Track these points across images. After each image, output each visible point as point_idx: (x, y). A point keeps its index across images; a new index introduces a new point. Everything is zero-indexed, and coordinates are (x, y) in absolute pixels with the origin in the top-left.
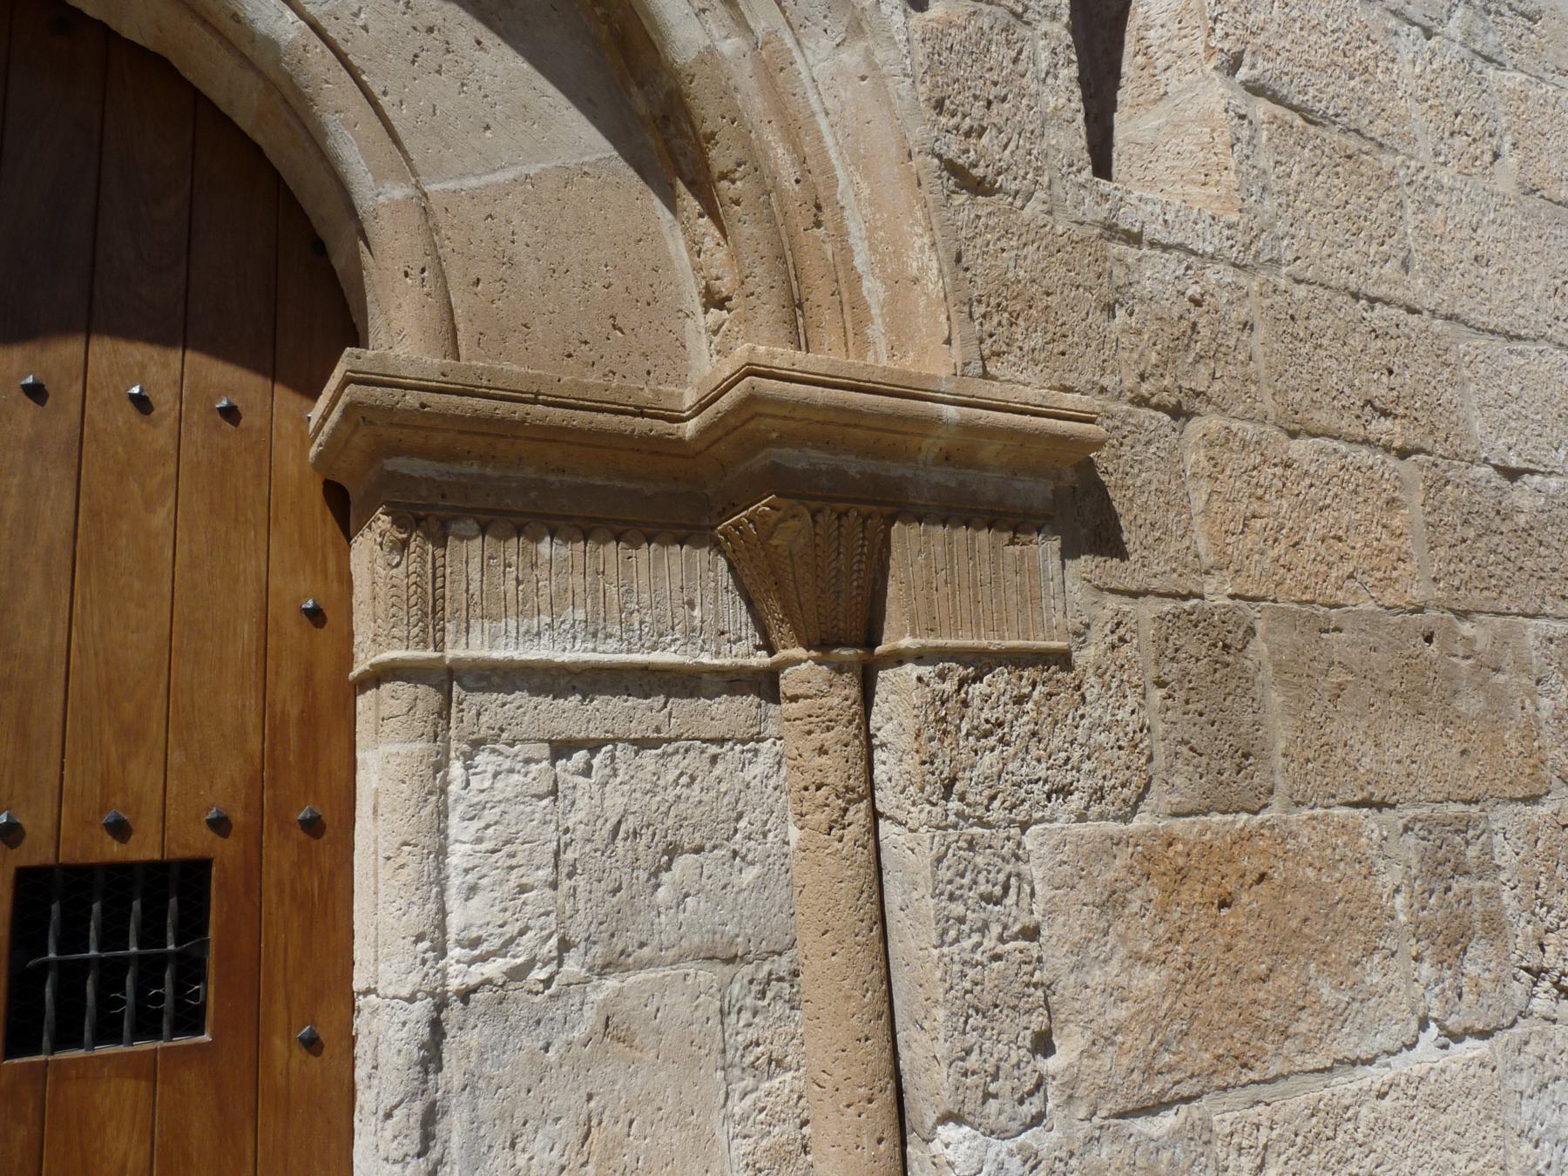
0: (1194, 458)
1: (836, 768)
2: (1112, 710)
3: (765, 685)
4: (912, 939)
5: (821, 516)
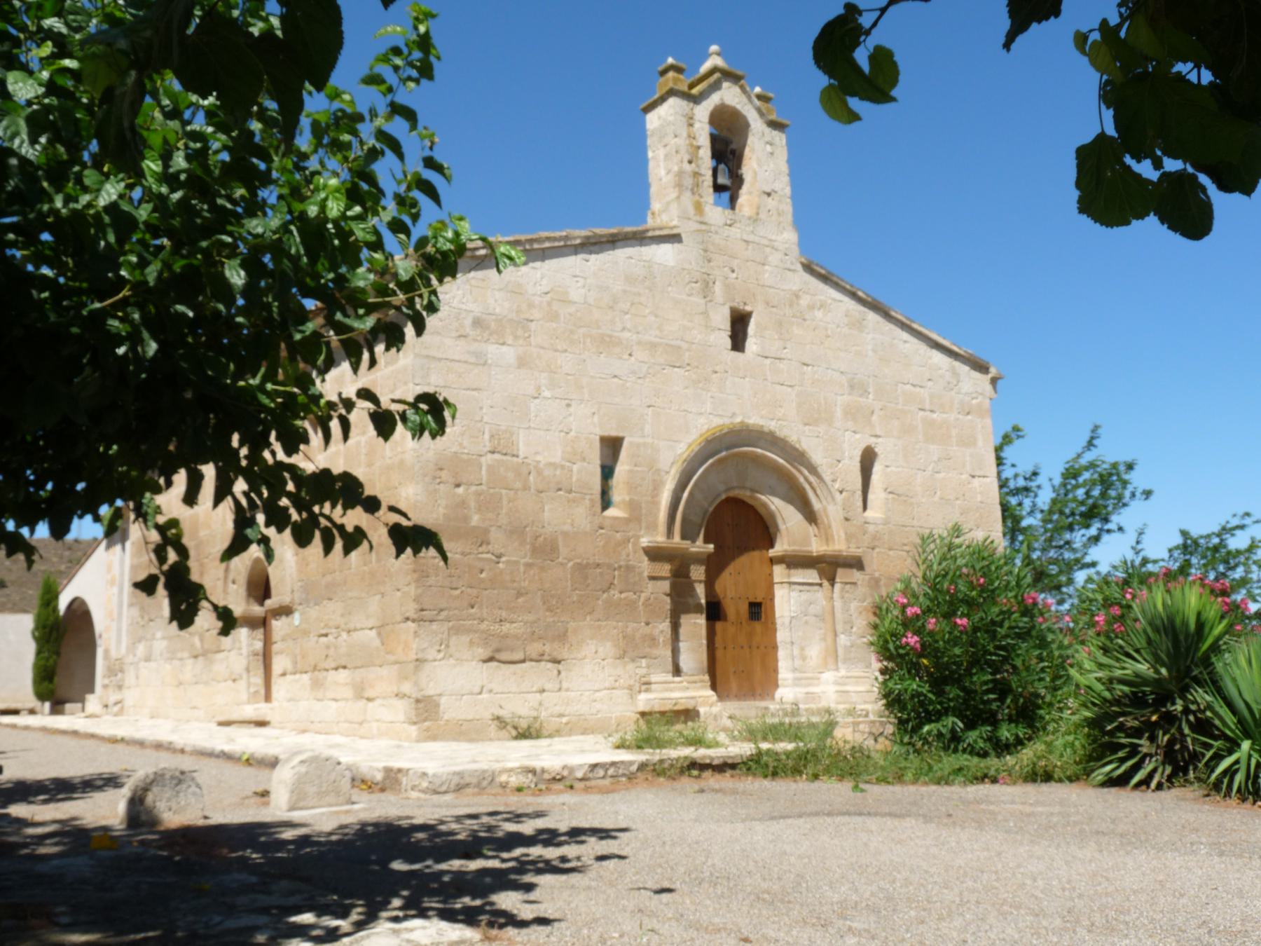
2: (862, 590)
3: (821, 585)
5: (829, 567)
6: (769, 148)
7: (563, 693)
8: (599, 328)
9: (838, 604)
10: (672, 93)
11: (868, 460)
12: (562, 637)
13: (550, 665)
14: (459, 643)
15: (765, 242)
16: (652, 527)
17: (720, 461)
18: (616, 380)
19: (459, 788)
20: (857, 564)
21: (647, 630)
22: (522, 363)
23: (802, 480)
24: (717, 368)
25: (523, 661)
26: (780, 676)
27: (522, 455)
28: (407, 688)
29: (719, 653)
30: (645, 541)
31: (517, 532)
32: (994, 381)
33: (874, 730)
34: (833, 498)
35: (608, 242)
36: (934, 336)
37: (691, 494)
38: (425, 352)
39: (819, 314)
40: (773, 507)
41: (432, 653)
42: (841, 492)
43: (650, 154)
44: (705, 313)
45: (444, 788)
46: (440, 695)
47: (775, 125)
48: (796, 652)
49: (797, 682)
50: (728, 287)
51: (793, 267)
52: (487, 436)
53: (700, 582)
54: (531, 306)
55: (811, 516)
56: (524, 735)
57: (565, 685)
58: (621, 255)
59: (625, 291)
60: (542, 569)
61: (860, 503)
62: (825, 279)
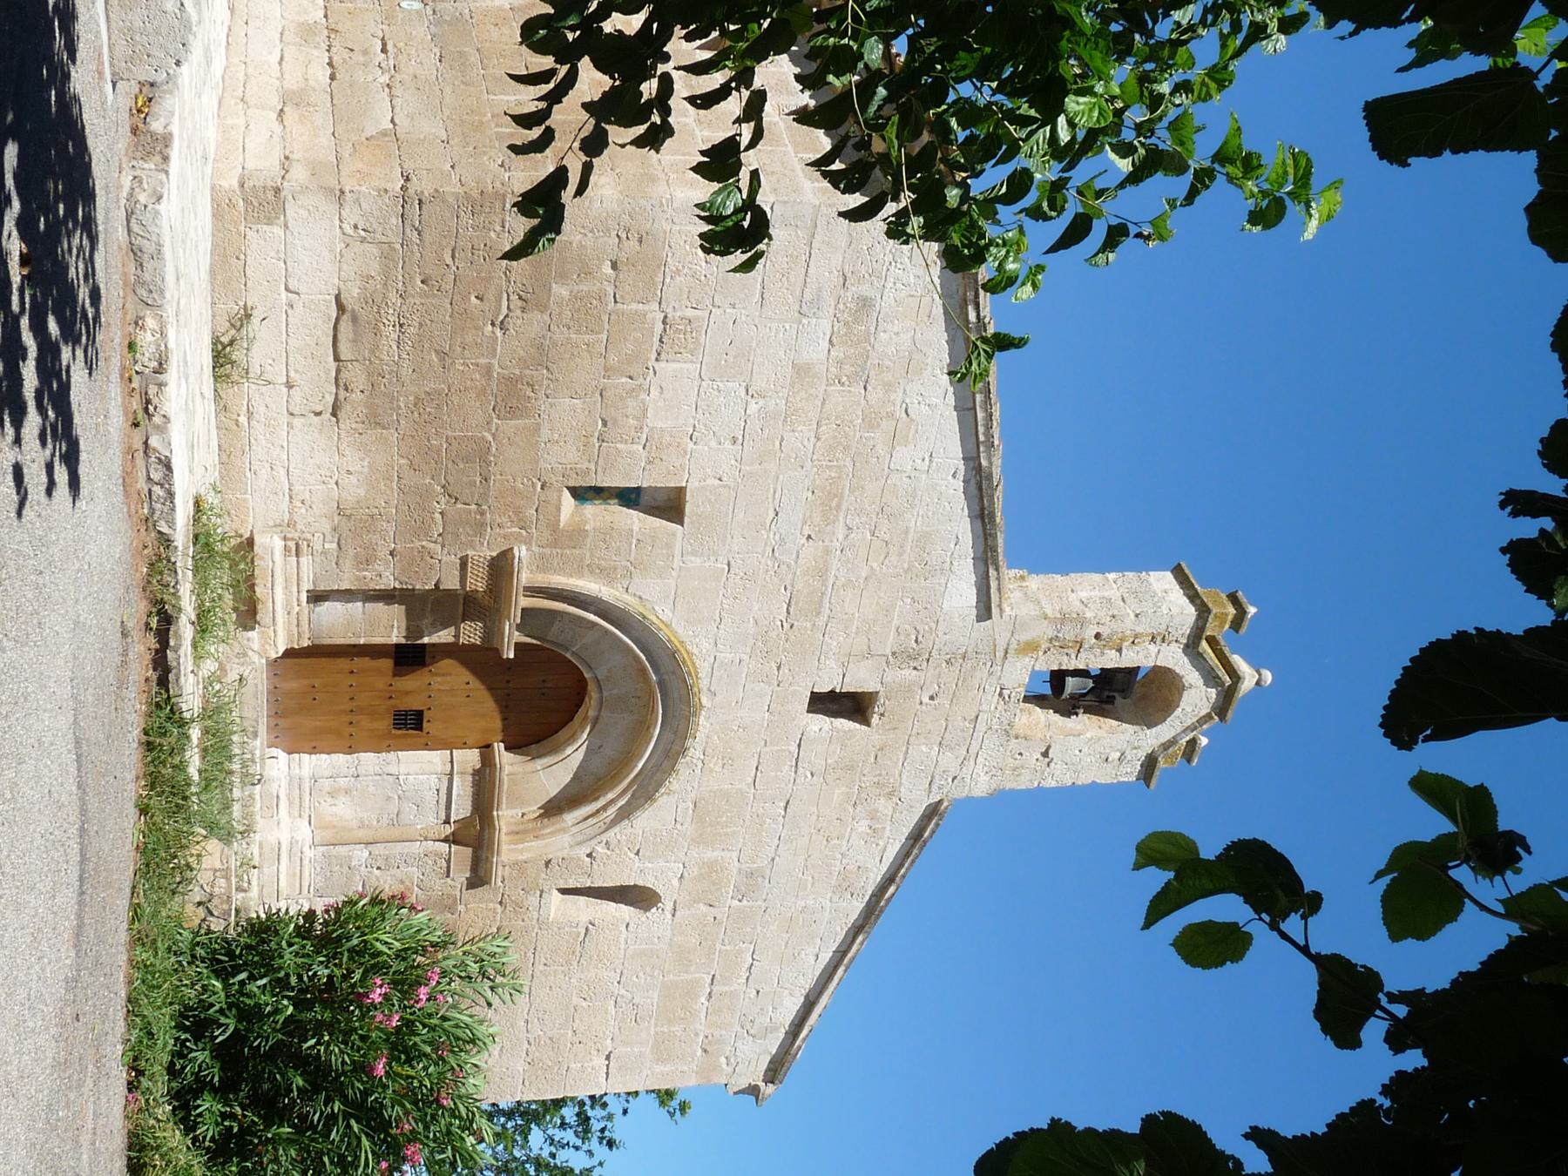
0: (491, 905)
1: (431, 835)
2: (438, 885)
3: (447, 822)
4: (399, 847)
5: (474, 836)
6: (1115, 755)
7: (285, 418)
8: (852, 490)
9: (416, 848)
10: (1203, 611)
11: (637, 897)
12: (374, 420)
13: (330, 399)
14: (368, 259)
15: (973, 750)
16: (543, 565)
17: (643, 670)
18: (772, 514)
19: (135, 252)
20: (478, 878)
21: (383, 552)
22: (802, 371)
23: (611, 796)
24: (785, 670)
25: (337, 359)
26: (305, 757)
27: (657, 366)
28: (298, 174)
29: (343, 663)
30: (521, 552)
31: (541, 355)
32: (753, 1090)
33: (216, 901)
34: (579, 844)
35: (982, 509)
36: (824, 1000)
37: (594, 624)
38: (821, 222)
39: (863, 827)
40: (569, 751)
41: (351, 215)
42: (589, 855)
43: (1112, 576)
44: (870, 654)
45: (135, 228)
46: (286, 226)
47: (1150, 765)
48: (342, 782)
49: (296, 782)
50: (908, 689)
51: (934, 788)
52: (690, 313)
53: (457, 636)
54: (889, 387)
55: (554, 808)
56: (221, 357)
57: (297, 422)
58: (962, 528)
59: (907, 533)
60: (483, 392)
61: (571, 884)
62: (916, 837)
